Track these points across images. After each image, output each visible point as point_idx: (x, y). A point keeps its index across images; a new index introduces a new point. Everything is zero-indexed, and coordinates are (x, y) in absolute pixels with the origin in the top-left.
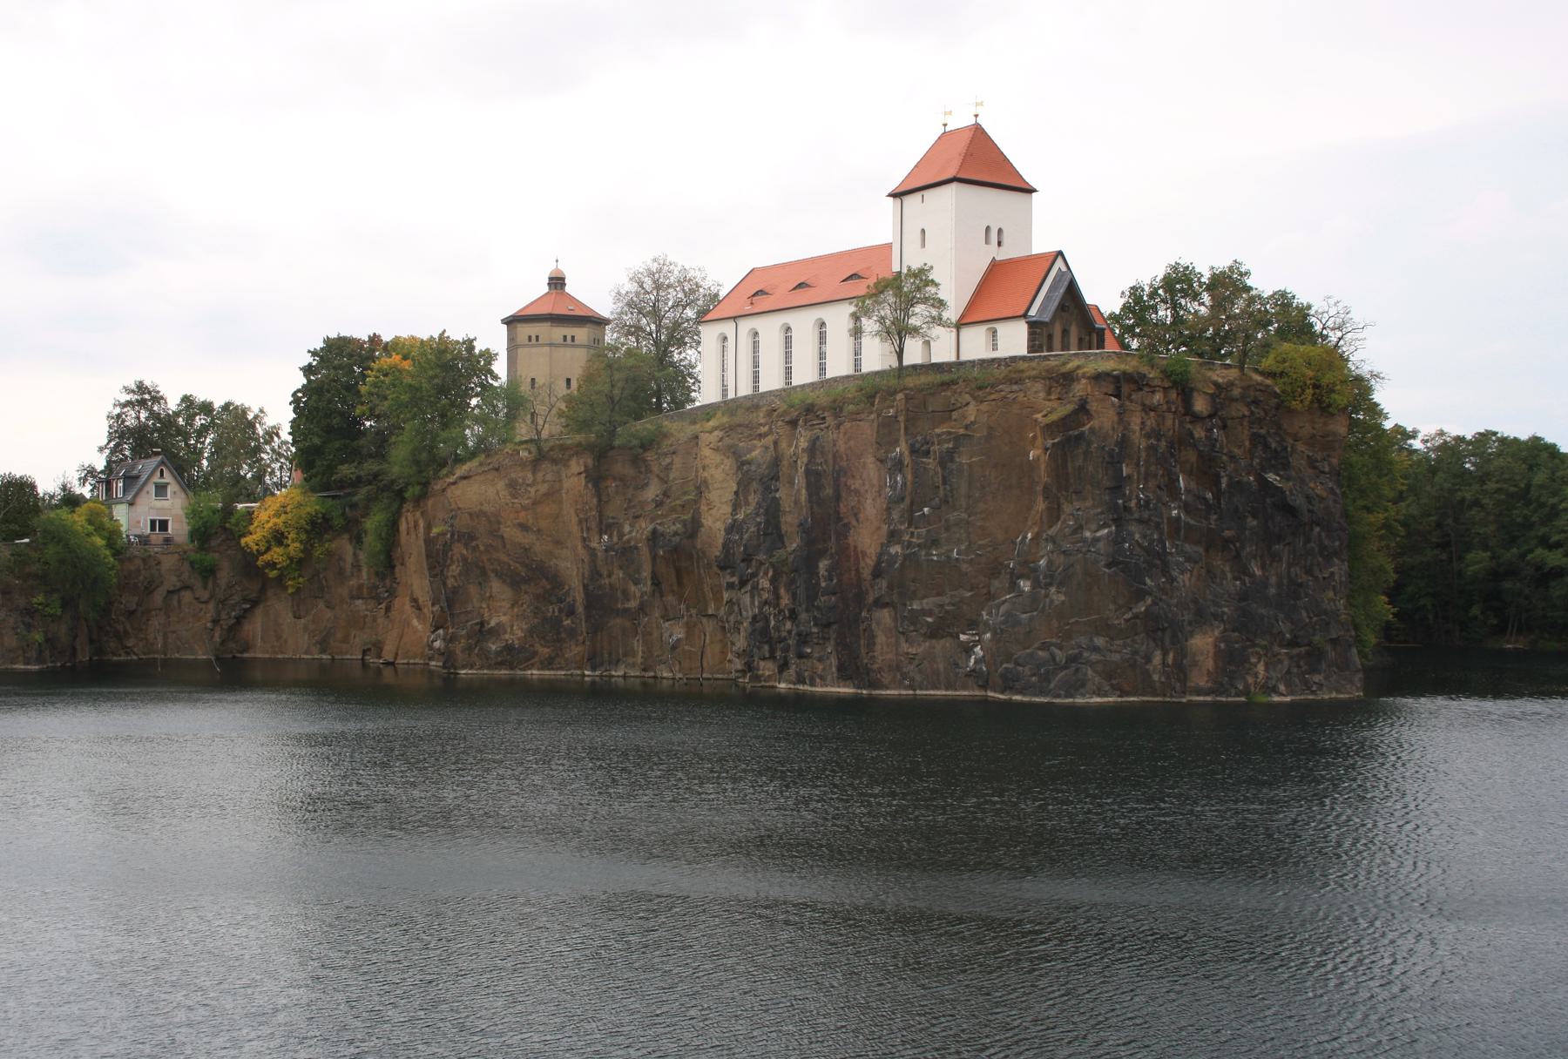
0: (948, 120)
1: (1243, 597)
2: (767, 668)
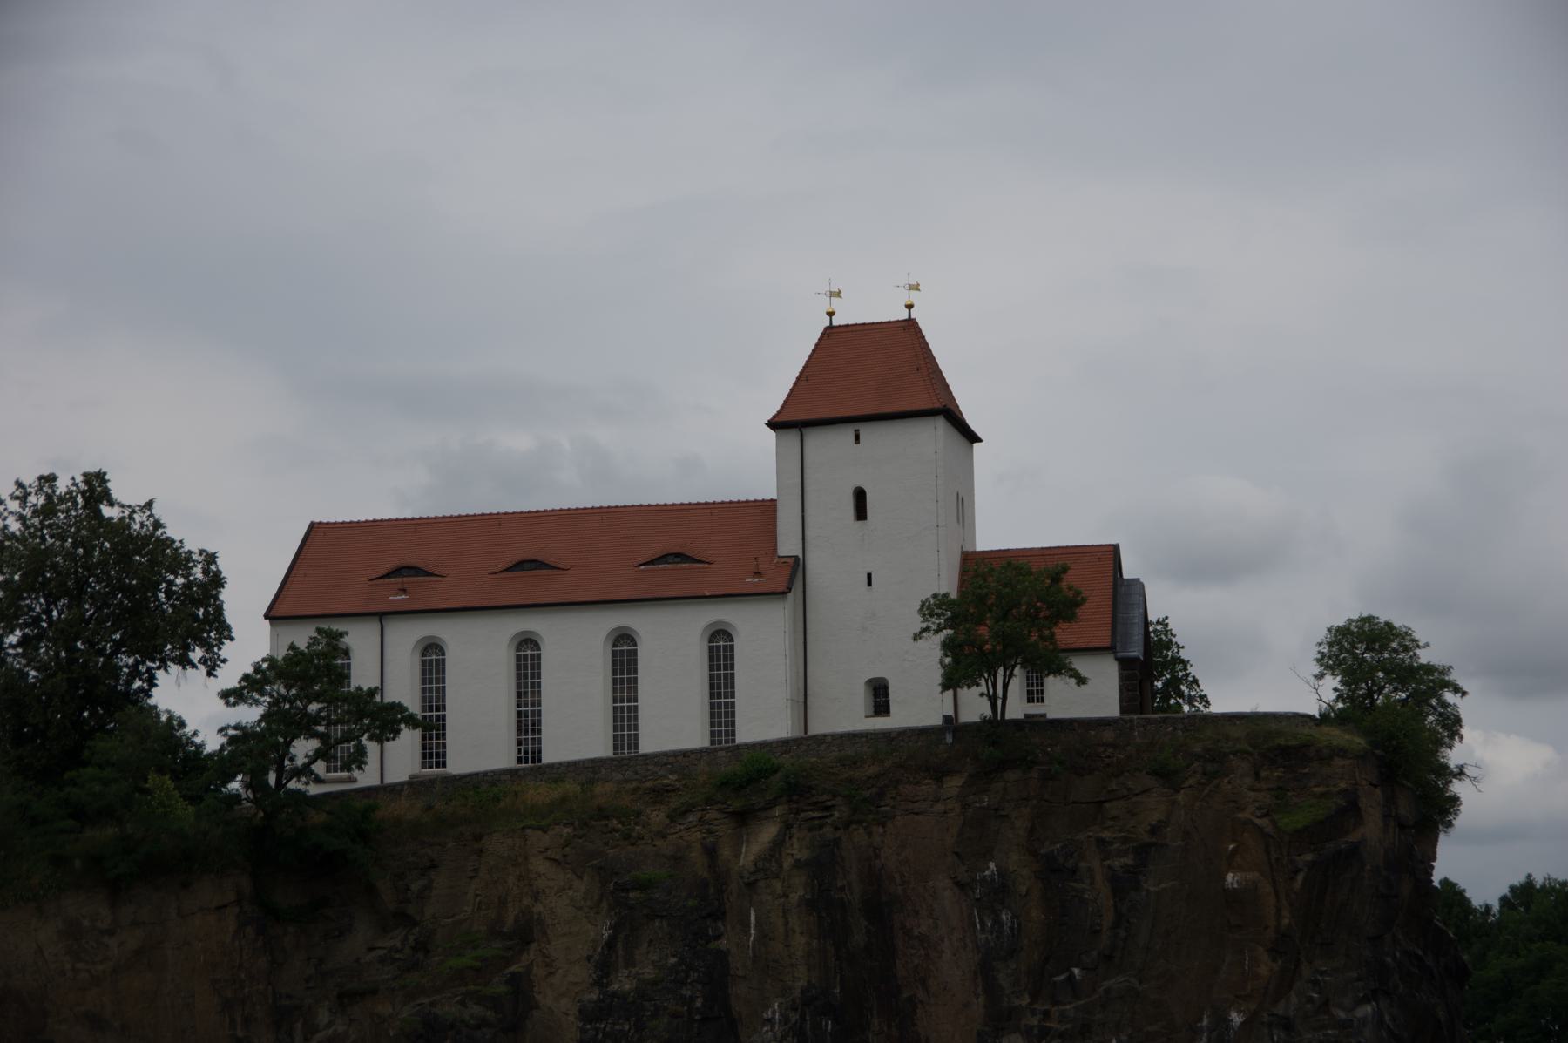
0: (836, 305)
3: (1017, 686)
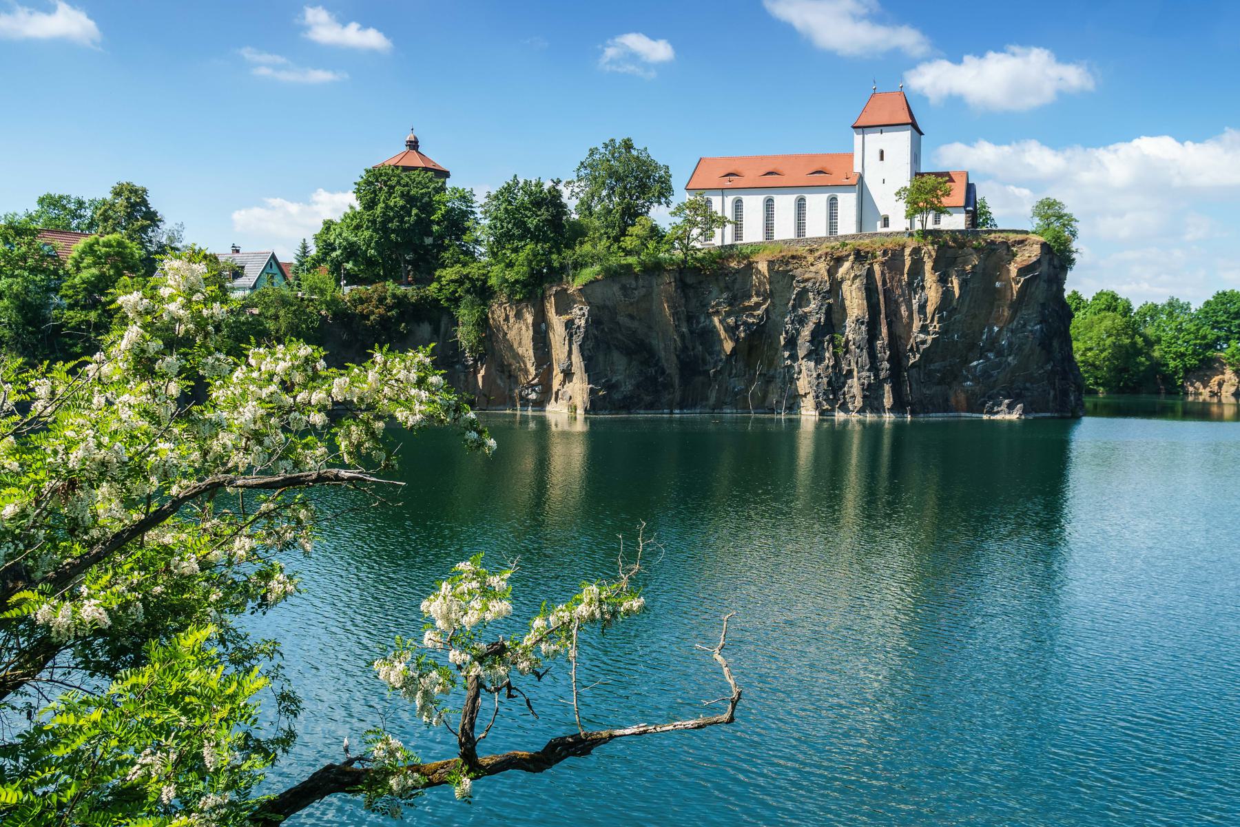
3: (931, 217)
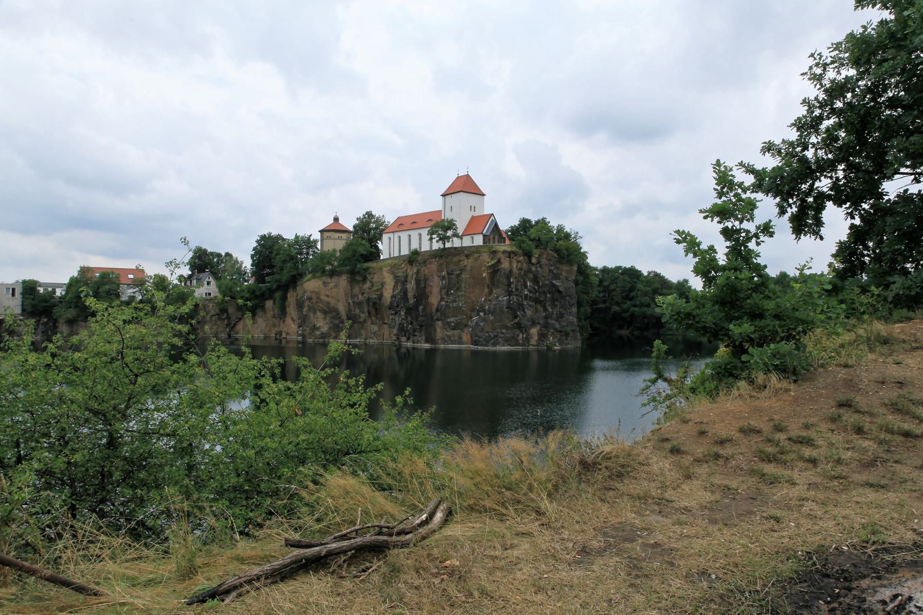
1: (546, 318)
2: (403, 339)
